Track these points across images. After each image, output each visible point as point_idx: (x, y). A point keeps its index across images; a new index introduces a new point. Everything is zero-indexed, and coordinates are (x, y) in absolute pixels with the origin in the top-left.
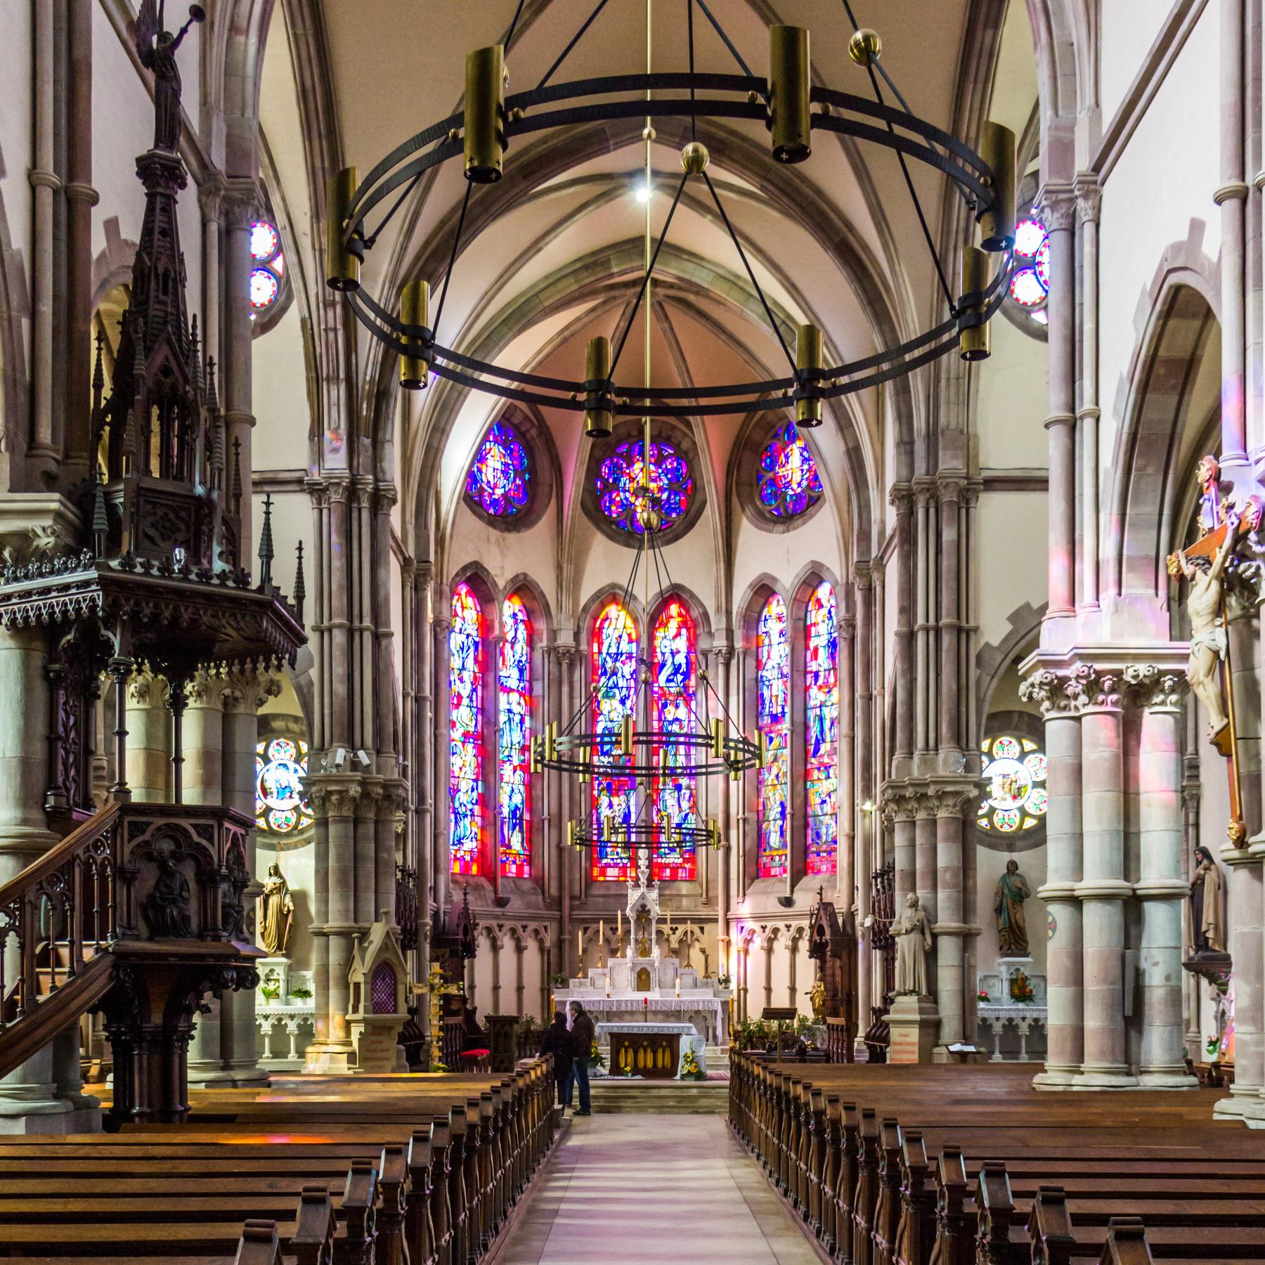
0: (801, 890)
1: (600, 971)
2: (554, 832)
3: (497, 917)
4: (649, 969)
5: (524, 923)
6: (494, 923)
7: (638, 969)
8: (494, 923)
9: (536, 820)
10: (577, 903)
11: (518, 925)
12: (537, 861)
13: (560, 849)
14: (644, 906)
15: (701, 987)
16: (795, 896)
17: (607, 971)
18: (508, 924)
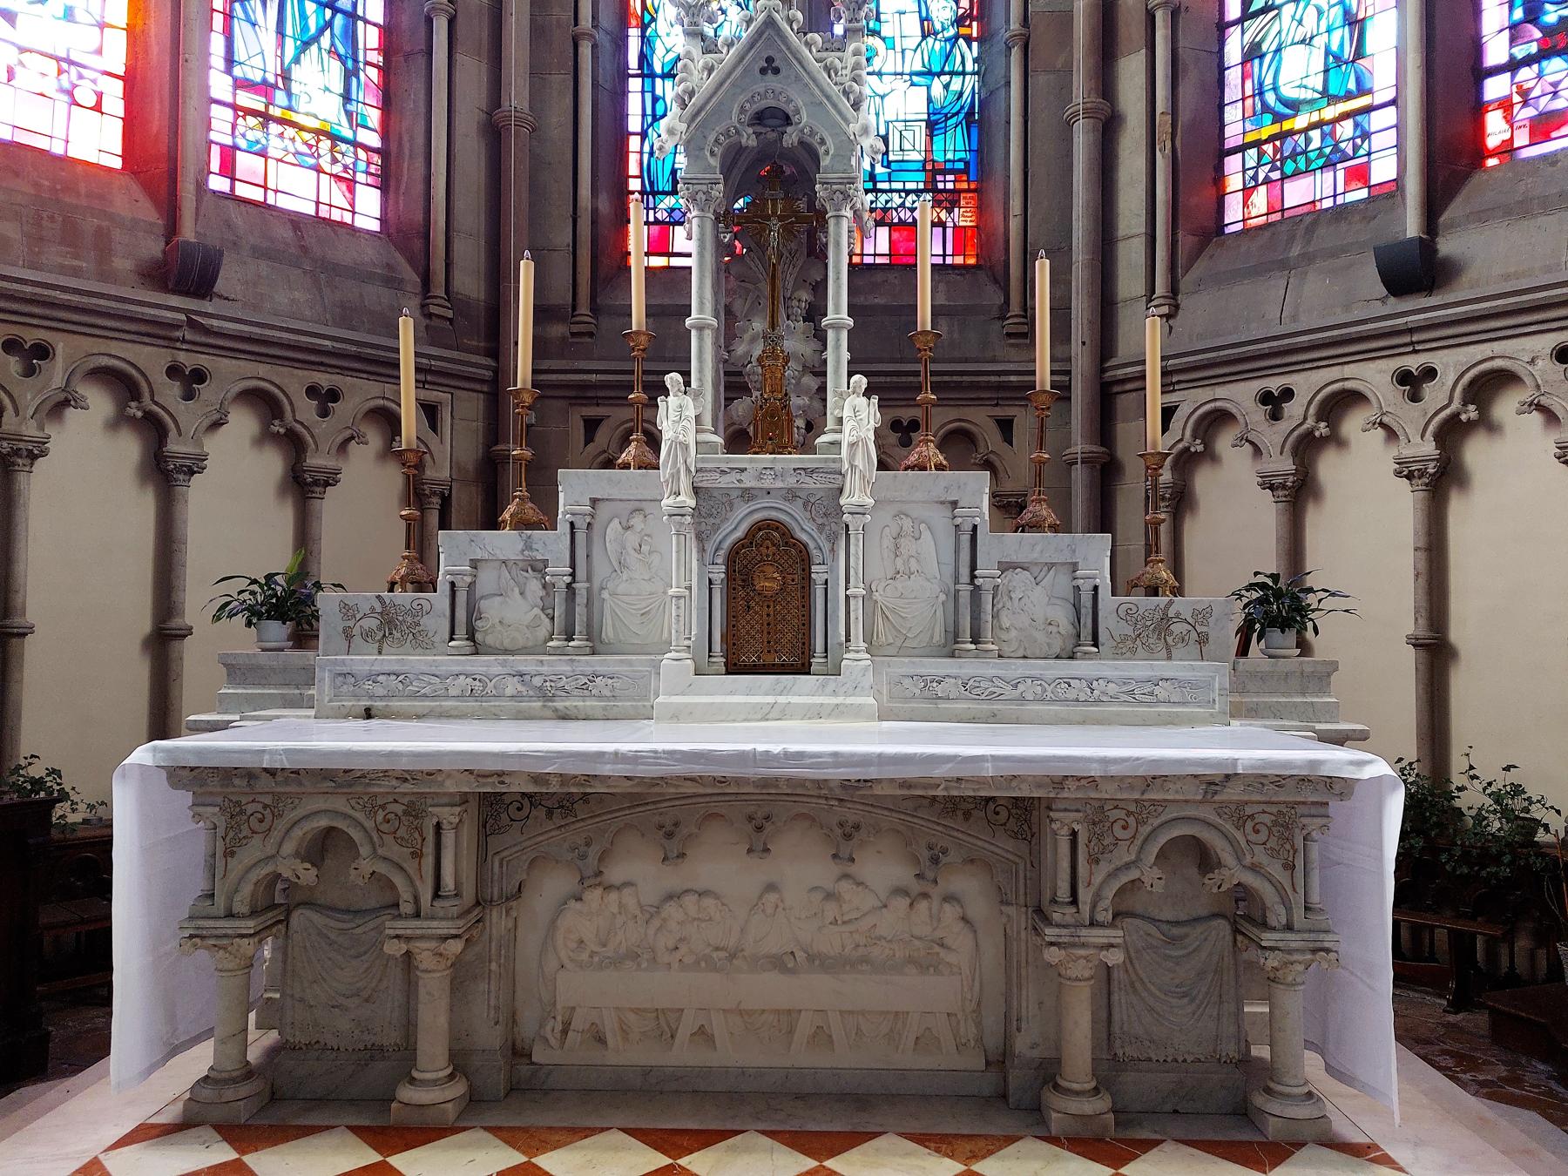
0: (1482, 216)
1: (504, 542)
2: (472, 71)
3: (159, 332)
4: (805, 530)
5: (324, 380)
6: (150, 360)
7: (735, 526)
8: (150, 360)
9: (405, 20)
10: (557, 330)
11: (292, 383)
12: (411, 170)
13: (494, 133)
14: (772, 118)
15: (1127, 648)
16: (1447, 246)
17: (552, 545)
18: (230, 373)
